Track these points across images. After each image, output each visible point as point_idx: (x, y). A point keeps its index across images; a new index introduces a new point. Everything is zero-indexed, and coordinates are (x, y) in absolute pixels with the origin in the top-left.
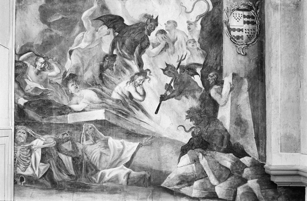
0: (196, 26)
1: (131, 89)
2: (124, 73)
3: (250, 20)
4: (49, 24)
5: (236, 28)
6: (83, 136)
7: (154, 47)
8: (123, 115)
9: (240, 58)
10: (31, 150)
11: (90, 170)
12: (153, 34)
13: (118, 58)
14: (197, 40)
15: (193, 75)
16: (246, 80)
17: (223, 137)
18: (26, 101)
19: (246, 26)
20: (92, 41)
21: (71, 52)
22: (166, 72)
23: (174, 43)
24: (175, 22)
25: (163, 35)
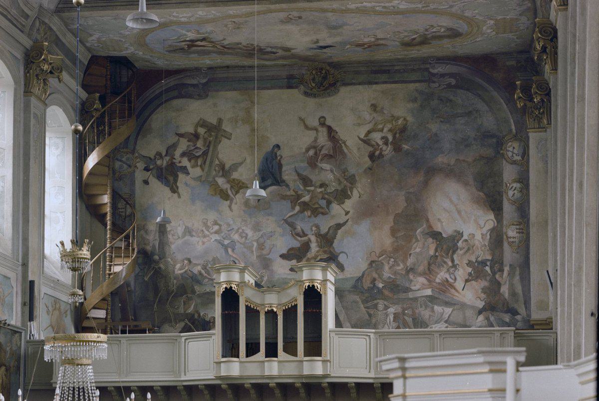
0: (486, 236)
1: (447, 276)
2: (443, 266)
3: (521, 231)
4: (397, 238)
5: (512, 236)
6: (419, 305)
7: (461, 250)
8: (443, 292)
9: (515, 255)
10: (387, 315)
11: (423, 325)
12: (460, 242)
13: (439, 258)
14: (487, 244)
15: (485, 267)
16: (518, 268)
17: (504, 304)
18: (383, 285)
19: (518, 235)
20: (423, 248)
21: (410, 254)
22: (469, 265)
23: (473, 247)
24: (473, 234)
25: (466, 243)
